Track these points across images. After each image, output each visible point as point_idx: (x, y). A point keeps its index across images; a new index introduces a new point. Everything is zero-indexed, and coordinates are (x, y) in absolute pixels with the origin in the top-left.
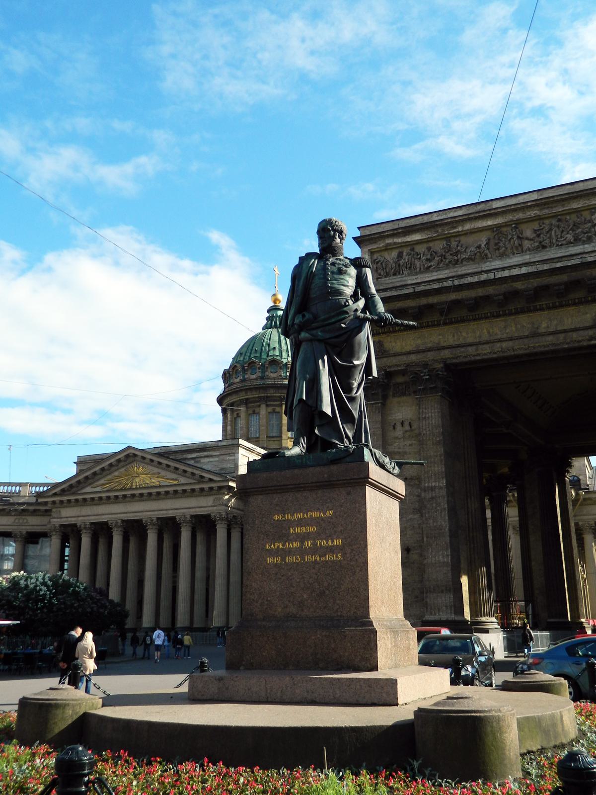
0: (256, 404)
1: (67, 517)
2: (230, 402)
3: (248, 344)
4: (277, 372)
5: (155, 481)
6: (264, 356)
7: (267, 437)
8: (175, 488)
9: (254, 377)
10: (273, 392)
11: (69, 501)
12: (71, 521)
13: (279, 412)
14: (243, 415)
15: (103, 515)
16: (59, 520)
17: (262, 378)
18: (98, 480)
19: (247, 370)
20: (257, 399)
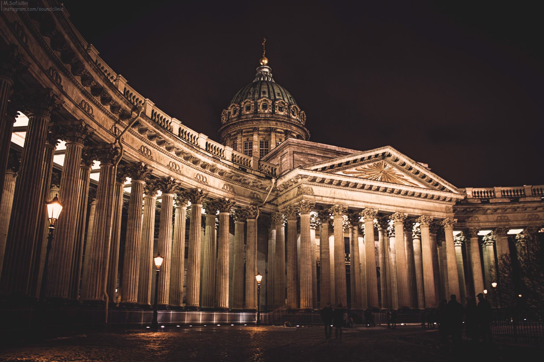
1: (322, 197)
4: (295, 116)
9: (282, 113)
16: (313, 197)
20: (282, 131)
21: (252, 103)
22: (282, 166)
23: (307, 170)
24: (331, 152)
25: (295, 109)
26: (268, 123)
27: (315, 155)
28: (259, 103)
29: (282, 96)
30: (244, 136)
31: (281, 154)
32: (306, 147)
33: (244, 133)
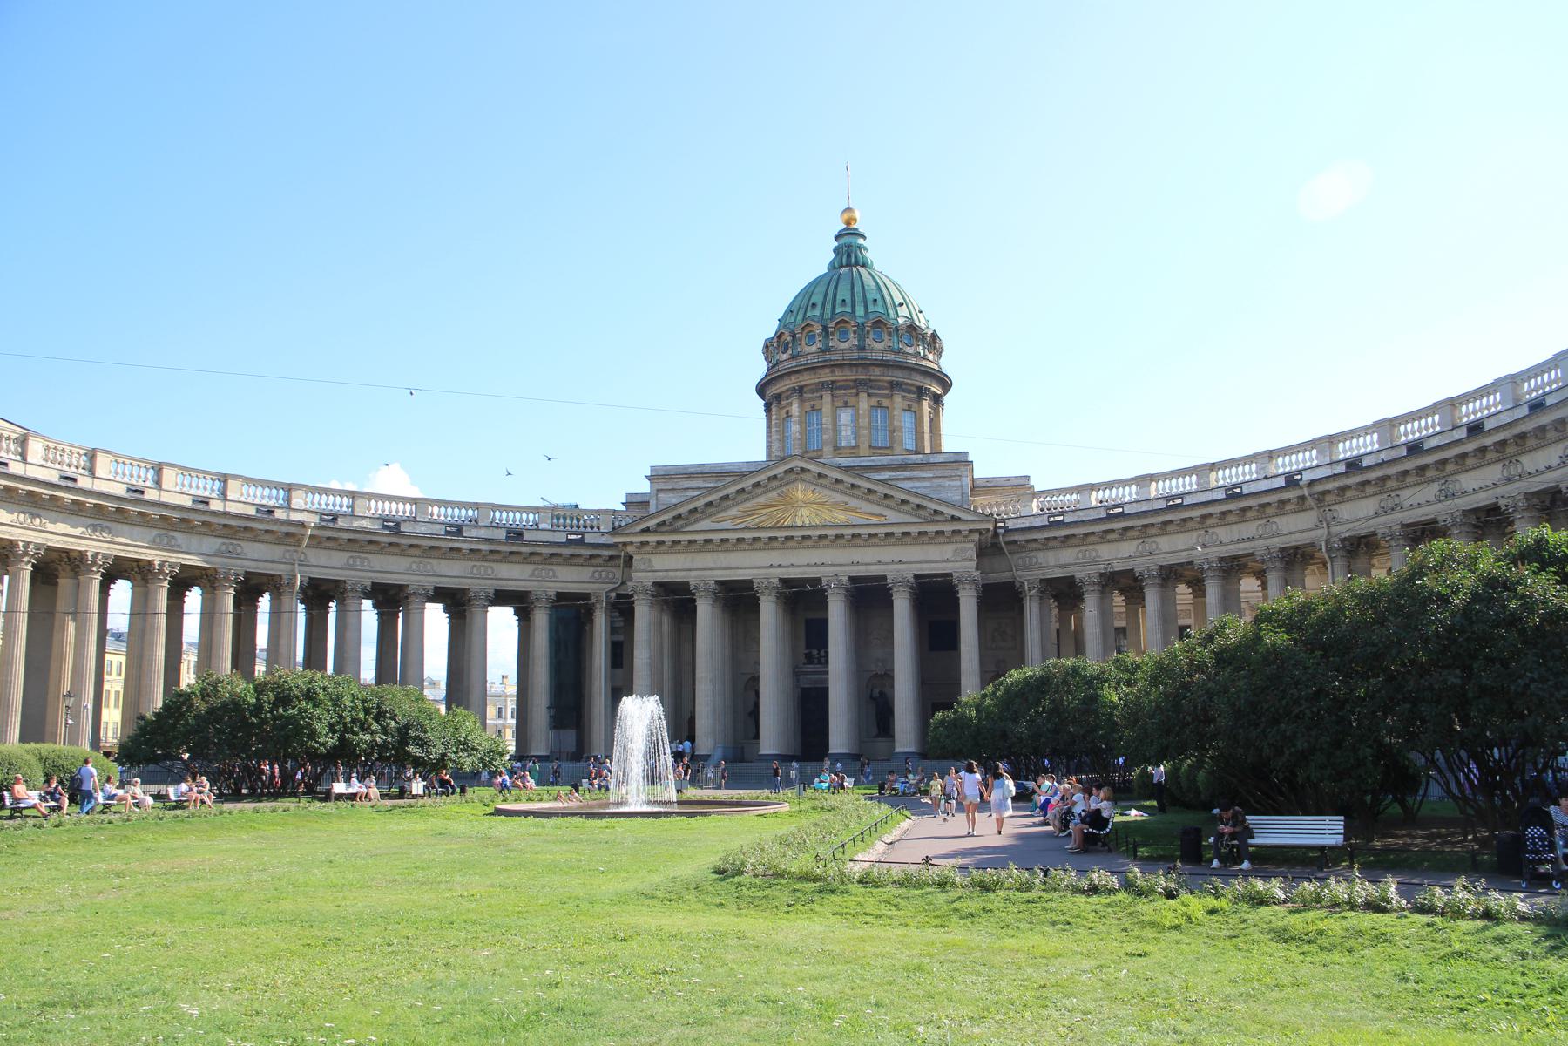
0: (850, 391)
1: (666, 571)
2: (799, 384)
3: (821, 289)
5: (841, 517)
6: (860, 311)
7: (870, 447)
8: (889, 530)
9: (844, 345)
10: (878, 373)
12: (676, 577)
13: (887, 408)
15: (741, 568)
16: (649, 574)
17: (862, 349)
18: (725, 509)
19: (832, 334)
20: (851, 384)
23: (627, 534)
27: (699, 488)
29: (850, 305)
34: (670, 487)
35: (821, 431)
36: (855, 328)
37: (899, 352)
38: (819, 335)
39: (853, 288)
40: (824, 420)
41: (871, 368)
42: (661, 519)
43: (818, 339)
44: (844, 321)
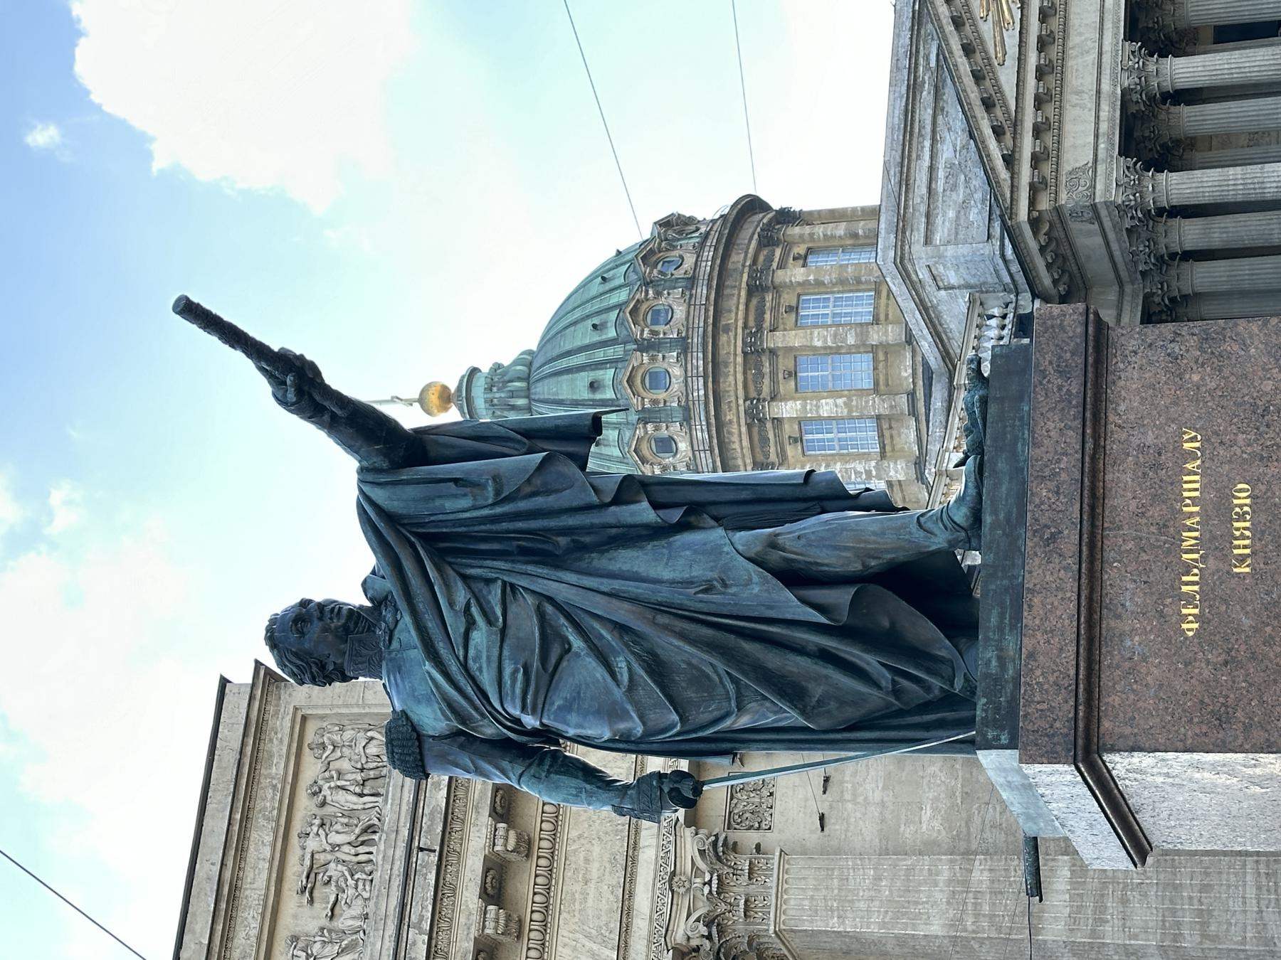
0: (768, 305)
1: (1097, 136)
2: (741, 402)
4: (682, 257)
6: (622, 296)
9: (680, 312)
10: (743, 255)
11: (1038, 132)
12: (1111, 120)
13: (809, 249)
14: (794, 339)
16: (1101, 168)
21: (645, 428)
22: (972, 282)
23: (1012, 192)
24: (913, 112)
25: (654, 259)
26: (726, 365)
27: (932, 169)
28: (643, 404)
29: (604, 316)
30: (783, 450)
31: (934, 288)
32: (906, 200)
33: (767, 455)
34: (923, 219)
35: (837, 351)
36: (651, 292)
37: (707, 234)
38: (653, 359)
39: (575, 323)
40: (818, 343)
41: (730, 266)
42: (988, 132)
43: (660, 365)
44: (634, 312)
